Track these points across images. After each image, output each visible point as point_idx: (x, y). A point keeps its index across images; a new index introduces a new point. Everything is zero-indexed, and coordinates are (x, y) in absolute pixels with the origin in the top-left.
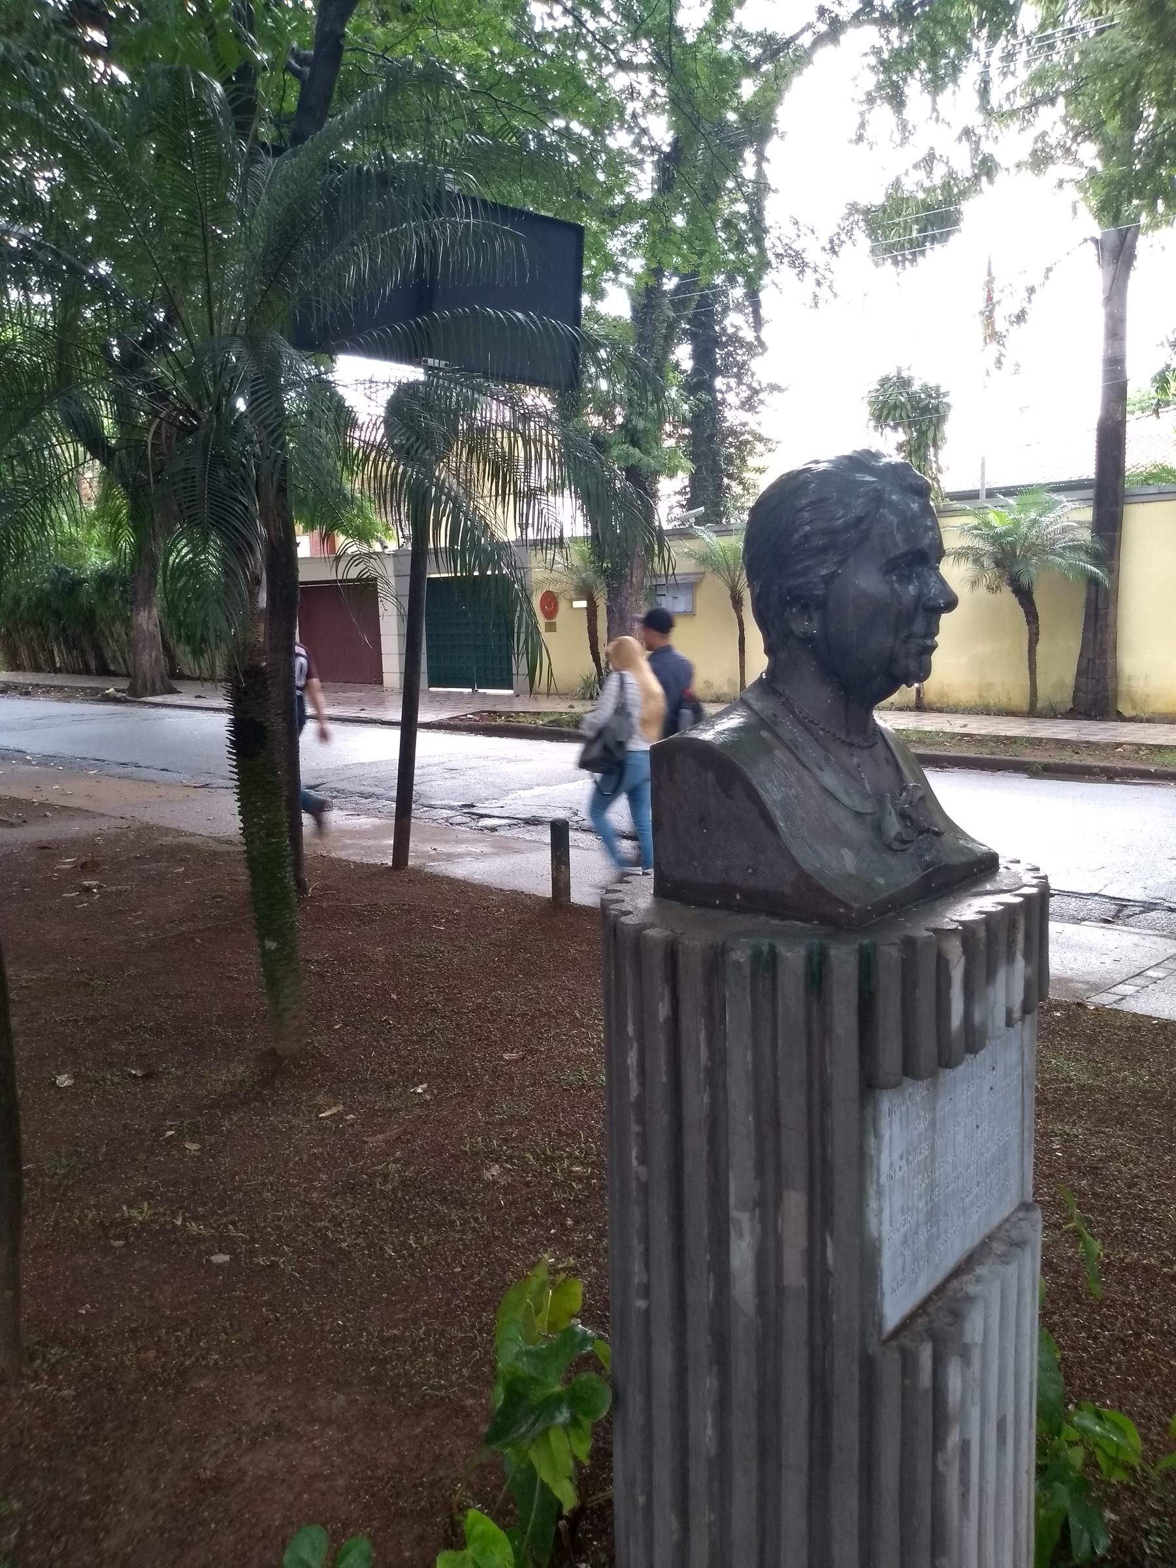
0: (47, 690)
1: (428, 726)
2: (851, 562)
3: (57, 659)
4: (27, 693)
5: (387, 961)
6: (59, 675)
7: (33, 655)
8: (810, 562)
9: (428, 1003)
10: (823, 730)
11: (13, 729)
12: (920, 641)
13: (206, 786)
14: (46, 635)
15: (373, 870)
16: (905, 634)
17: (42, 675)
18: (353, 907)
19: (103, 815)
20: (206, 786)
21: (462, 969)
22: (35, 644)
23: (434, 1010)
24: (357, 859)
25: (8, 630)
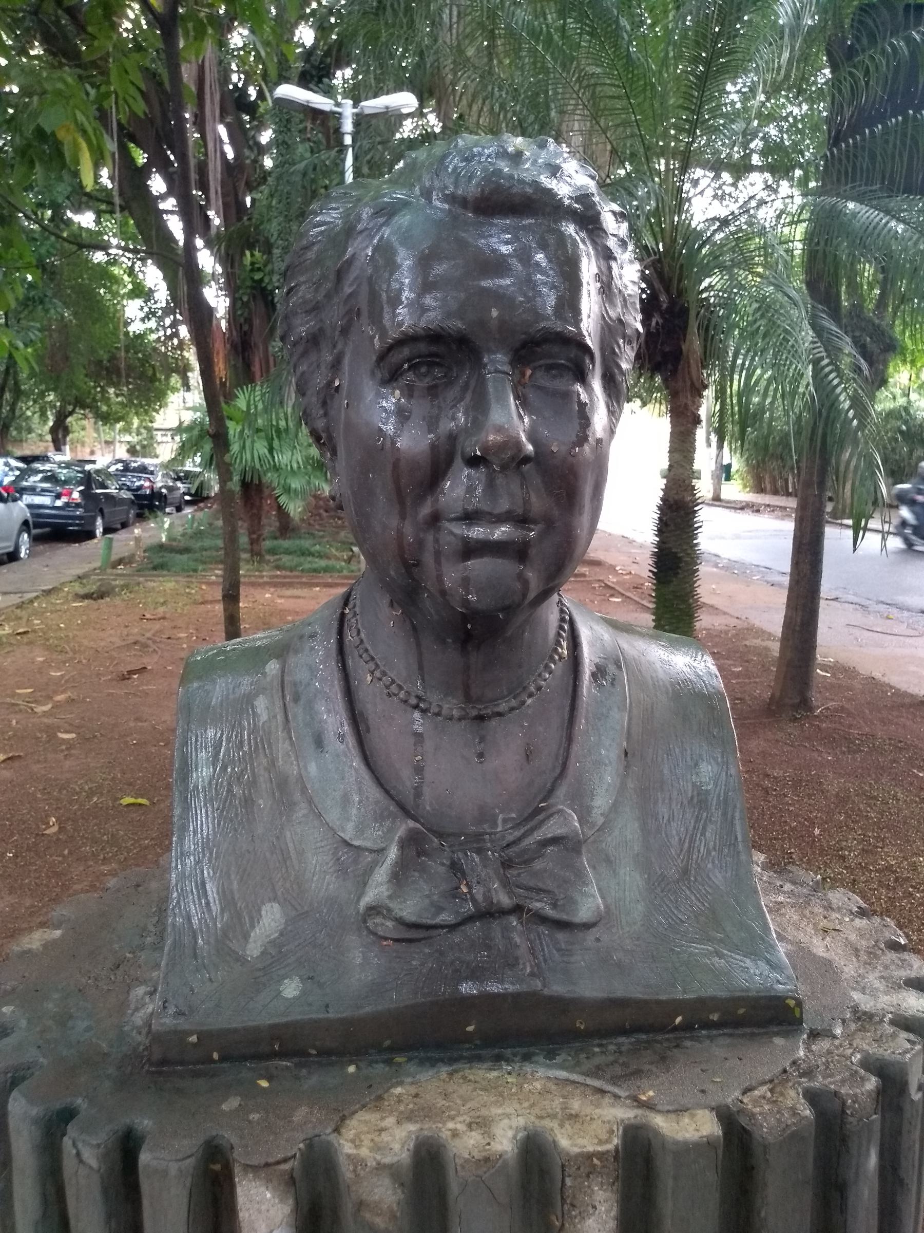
0: (772, 508)
1: (245, 584)
2: (346, 361)
3: (790, 485)
4: (758, 511)
5: (837, 795)
6: (790, 499)
7: (774, 481)
8: (305, 368)
9: (842, 849)
10: (372, 673)
11: (723, 538)
12: (459, 529)
13: (836, 599)
14: (784, 467)
15: (907, 700)
16: (426, 510)
17: (776, 498)
18: (849, 734)
19: (725, 613)
20: (836, 599)
21: (905, 823)
22: (776, 472)
23: (843, 858)
24: (903, 687)
25: (758, 462)
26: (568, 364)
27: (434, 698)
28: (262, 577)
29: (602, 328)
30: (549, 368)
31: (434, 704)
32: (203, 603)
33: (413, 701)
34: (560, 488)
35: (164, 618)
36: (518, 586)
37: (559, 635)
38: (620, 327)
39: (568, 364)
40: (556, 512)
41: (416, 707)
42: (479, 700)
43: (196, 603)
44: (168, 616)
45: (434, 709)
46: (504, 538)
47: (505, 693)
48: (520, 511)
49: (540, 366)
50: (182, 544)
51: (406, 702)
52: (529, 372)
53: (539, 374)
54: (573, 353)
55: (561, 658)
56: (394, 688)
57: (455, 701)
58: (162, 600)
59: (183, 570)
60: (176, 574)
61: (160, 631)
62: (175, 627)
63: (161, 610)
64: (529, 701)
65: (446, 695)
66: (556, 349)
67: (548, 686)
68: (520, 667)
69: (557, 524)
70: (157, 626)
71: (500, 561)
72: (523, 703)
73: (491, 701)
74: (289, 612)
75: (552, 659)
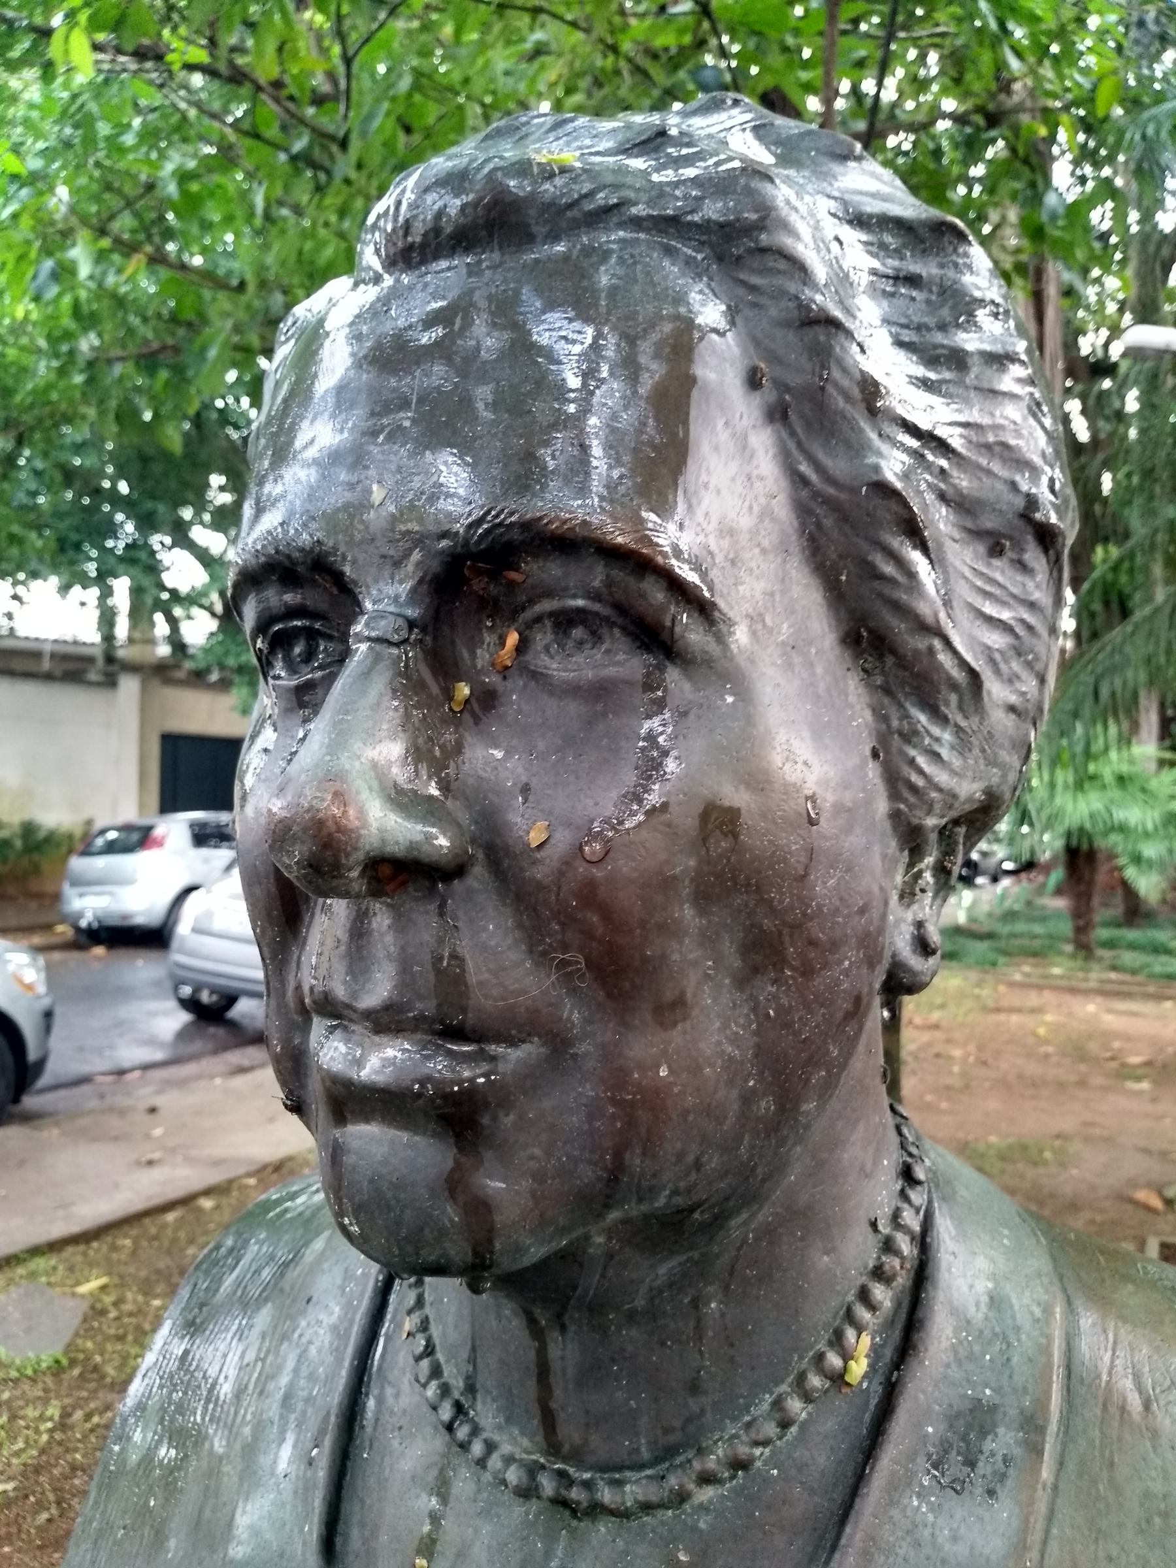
26: (597, 607)
27: (486, 1413)
28: (1086, 980)
29: (802, 510)
30: (565, 621)
31: (485, 1435)
32: (998, 1010)
33: (446, 1413)
34: (565, 947)
35: (936, 1027)
36: (451, 1214)
37: (850, 1317)
38: (885, 511)
39: (597, 607)
40: (573, 1014)
41: (449, 1428)
42: (577, 1456)
43: (986, 1010)
44: (944, 1023)
45: (477, 1448)
46: (381, 1079)
47: (645, 1454)
48: (426, 1007)
49: (538, 619)
50: (986, 928)
51: (435, 1408)
52: (513, 639)
53: (542, 637)
54: (597, 574)
55: (838, 1379)
56: (425, 1363)
57: (525, 1442)
58: (938, 1001)
59: (977, 963)
60: (969, 967)
61: (929, 1045)
62: (949, 1041)
63: (936, 1016)
64: (707, 1494)
65: (508, 1420)
66: (551, 570)
67: (772, 1461)
68: (694, 1388)
69: (583, 1048)
70: (926, 1037)
71: (404, 1136)
72: (682, 1497)
73: (603, 1468)
74: (1116, 1035)
75: (801, 1378)
